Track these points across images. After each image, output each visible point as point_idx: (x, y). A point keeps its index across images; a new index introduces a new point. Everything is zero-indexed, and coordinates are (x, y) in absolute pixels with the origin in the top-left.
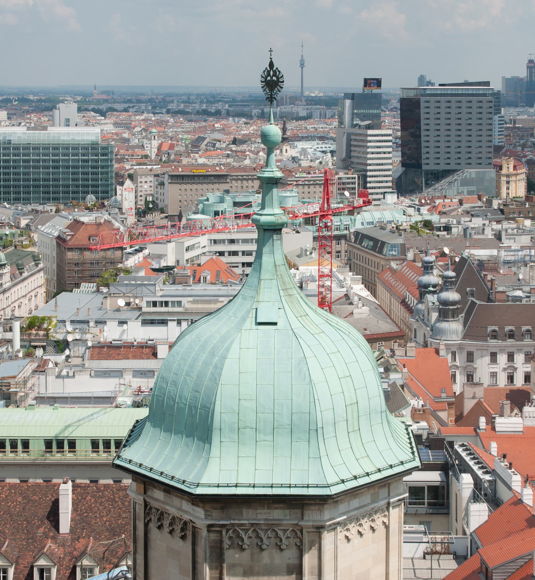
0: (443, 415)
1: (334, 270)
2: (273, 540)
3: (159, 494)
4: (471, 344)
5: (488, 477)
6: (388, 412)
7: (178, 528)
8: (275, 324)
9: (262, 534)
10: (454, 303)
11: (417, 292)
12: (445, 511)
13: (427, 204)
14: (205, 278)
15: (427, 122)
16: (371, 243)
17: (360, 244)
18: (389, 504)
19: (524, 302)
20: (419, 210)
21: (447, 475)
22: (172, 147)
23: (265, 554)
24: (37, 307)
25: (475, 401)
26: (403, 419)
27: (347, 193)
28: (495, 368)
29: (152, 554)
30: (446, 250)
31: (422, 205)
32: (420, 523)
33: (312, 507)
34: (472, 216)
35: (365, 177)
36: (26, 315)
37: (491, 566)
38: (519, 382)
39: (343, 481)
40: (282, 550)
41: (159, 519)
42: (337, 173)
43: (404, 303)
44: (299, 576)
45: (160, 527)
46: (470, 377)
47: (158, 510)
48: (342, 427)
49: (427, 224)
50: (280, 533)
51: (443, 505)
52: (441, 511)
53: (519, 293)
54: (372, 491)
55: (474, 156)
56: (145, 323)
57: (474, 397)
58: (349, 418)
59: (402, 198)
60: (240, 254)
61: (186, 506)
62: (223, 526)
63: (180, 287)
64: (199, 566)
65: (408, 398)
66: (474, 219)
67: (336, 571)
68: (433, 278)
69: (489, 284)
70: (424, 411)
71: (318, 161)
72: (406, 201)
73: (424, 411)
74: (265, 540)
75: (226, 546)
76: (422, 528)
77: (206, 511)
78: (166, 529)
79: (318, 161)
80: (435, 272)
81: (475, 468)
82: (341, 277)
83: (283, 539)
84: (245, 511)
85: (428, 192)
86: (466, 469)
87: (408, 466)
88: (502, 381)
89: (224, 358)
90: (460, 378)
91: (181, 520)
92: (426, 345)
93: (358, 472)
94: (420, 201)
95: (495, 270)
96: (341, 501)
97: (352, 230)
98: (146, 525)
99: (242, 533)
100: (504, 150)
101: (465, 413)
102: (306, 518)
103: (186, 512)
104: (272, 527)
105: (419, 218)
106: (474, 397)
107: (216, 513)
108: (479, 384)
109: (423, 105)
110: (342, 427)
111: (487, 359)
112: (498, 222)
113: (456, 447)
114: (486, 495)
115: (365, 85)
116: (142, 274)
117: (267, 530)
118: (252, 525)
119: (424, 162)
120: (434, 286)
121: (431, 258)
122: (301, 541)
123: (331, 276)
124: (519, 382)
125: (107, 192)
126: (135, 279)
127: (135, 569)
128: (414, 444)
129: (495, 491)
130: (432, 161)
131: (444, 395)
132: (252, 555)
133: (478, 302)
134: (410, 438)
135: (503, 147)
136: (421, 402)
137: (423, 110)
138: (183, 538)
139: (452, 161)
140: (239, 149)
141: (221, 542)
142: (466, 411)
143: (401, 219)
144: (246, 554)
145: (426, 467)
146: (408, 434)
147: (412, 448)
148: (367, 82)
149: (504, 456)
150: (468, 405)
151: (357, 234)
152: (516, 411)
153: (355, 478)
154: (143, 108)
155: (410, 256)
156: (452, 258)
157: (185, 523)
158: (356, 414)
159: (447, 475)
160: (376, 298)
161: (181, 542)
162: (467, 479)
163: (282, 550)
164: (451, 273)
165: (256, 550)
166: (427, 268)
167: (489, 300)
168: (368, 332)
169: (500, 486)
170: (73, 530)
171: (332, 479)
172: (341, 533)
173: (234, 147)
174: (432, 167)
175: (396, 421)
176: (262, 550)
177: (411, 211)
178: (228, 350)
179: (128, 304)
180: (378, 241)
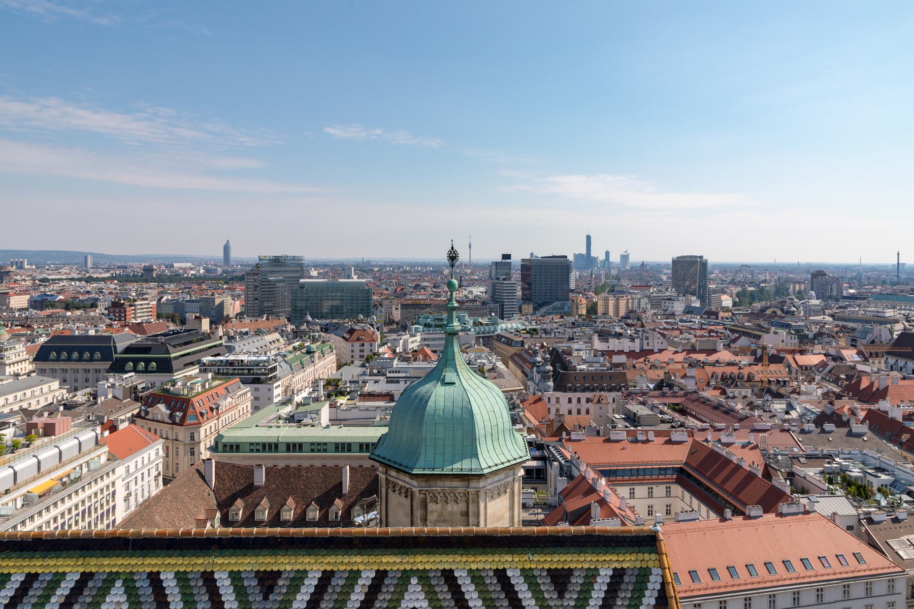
0: (544, 430)
2: (453, 498)
3: (393, 473)
4: (559, 394)
5: (567, 464)
7: (403, 491)
8: (454, 383)
9: (447, 495)
10: (549, 371)
11: (530, 366)
14: (419, 358)
20: (531, 323)
22: (402, 289)
23: (449, 505)
24: (332, 373)
26: (523, 433)
27: (493, 314)
29: (389, 505)
30: (545, 344)
32: (532, 488)
33: (474, 481)
35: (503, 305)
36: (326, 377)
41: (394, 487)
42: (488, 304)
43: (523, 372)
44: (466, 517)
45: (394, 491)
46: (558, 410)
47: (393, 482)
48: (489, 438)
50: (457, 494)
51: (544, 478)
54: (505, 472)
56: (388, 382)
58: (493, 433)
59: (522, 317)
61: (408, 479)
62: (427, 491)
63: (406, 363)
64: (414, 512)
68: (539, 359)
74: (449, 498)
75: (428, 501)
76: (532, 491)
77: (418, 482)
78: (397, 492)
80: (539, 355)
81: (560, 459)
84: (438, 482)
86: (556, 460)
87: (524, 459)
89: (427, 401)
91: (405, 487)
92: (534, 394)
93: (497, 462)
95: (570, 354)
97: (496, 333)
98: (387, 490)
99: (437, 494)
103: (408, 483)
105: (531, 327)
107: (423, 484)
110: (489, 438)
111: (567, 400)
114: (566, 473)
116: (386, 356)
117: (450, 493)
120: (539, 362)
121: (537, 348)
122: (468, 499)
125: (368, 313)
126: (383, 359)
127: (381, 513)
129: (571, 471)
131: (544, 421)
132: (442, 506)
138: (406, 497)
140: (437, 290)
141: (426, 499)
144: (439, 506)
145: (534, 458)
151: (498, 335)
154: (388, 269)
155: (526, 346)
156: (548, 348)
157: (407, 489)
160: (508, 368)
161: (405, 499)
163: (458, 503)
164: (548, 356)
165: (444, 503)
166: (535, 353)
169: (574, 468)
170: (350, 492)
173: (435, 290)
175: (517, 435)
176: (448, 503)
177: (526, 323)
178: (430, 397)
179: (379, 372)
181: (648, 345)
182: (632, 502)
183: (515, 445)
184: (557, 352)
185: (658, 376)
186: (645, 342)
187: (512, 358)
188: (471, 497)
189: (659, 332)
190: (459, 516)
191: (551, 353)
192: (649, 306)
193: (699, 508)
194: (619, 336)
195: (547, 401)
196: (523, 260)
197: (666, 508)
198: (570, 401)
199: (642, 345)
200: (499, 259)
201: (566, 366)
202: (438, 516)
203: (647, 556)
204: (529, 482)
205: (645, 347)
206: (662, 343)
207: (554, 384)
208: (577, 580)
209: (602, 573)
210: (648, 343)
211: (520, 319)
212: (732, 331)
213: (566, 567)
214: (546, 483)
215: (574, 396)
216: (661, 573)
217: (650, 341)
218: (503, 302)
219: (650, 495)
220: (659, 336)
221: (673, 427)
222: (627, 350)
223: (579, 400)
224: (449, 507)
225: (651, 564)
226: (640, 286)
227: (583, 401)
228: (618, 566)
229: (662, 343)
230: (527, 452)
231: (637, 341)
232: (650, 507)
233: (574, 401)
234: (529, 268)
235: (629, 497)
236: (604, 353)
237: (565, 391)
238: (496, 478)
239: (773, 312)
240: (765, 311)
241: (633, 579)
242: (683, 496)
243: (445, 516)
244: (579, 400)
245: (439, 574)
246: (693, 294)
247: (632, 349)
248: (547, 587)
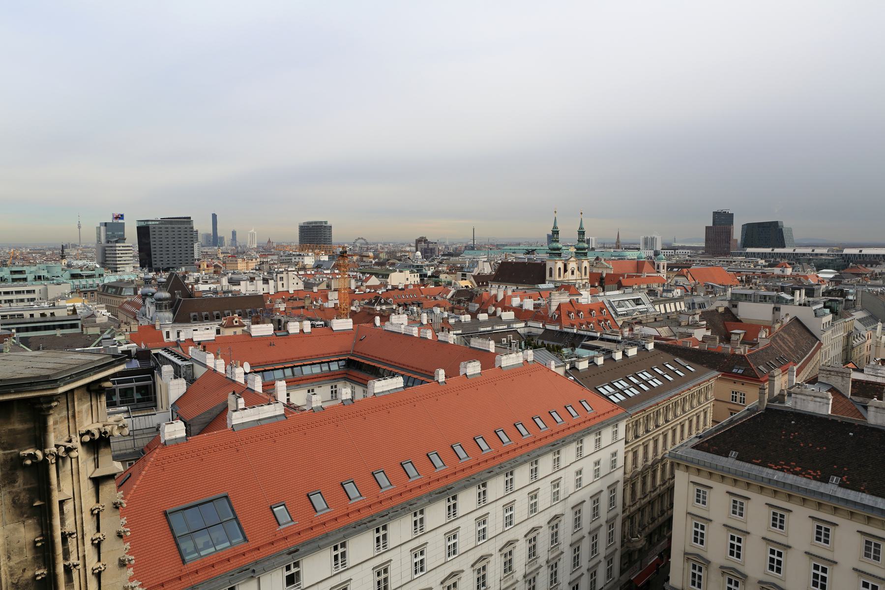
12: (153, 404)
52: (149, 405)
60: (26, 301)
180: (118, 287)
181: (283, 287)
186: (280, 283)
199: (276, 287)
205: (280, 289)
206: (297, 284)
210: (283, 284)
217: (285, 282)
229: (297, 284)
231: (271, 282)
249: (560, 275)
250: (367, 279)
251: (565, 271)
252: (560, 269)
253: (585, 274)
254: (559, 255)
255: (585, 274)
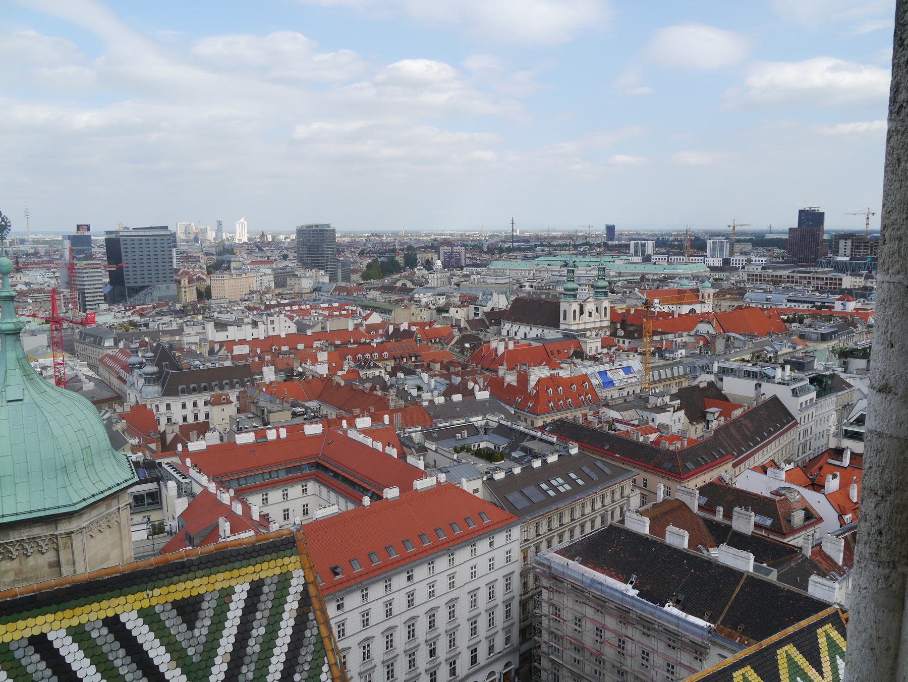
0: (153, 446)
1: (65, 359)
2: (36, 549)
6: (113, 450)
9: (26, 546)
13: (130, 309)
15: (126, 254)
16: (92, 339)
17: (84, 339)
18: (119, 508)
19: (201, 367)
21: (159, 484)
23: (30, 559)
25: (174, 434)
28: (184, 412)
31: (127, 310)
33: (63, 521)
34: (163, 315)
37: (192, 535)
38: (202, 418)
39: (84, 500)
40: (43, 554)
46: (169, 420)
48: (80, 465)
49: (132, 323)
50: (41, 543)
51: (158, 503)
53: (198, 363)
54: (106, 503)
55: (161, 275)
57: (173, 432)
65: (128, 439)
66: (164, 318)
67: (85, 559)
69: (177, 359)
70: (140, 446)
71: (46, 285)
72: (115, 308)
73: (140, 446)
79: (46, 285)
81: (177, 476)
82: (71, 364)
83: (43, 546)
84: (11, 533)
85: (131, 301)
86: (172, 478)
88: (191, 420)
90: (163, 421)
93: (95, 491)
94: (125, 308)
96: (85, 513)
99: (11, 549)
100: (181, 271)
101: (168, 443)
102: (59, 529)
104: (33, 540)
106: (173, 432)
108: (176, 423)
109: (122, 243)
110: (80, 465)
112: (181, 318)
113: (163, 465)
115: (78, 230)
117: (30, 542)
118: (18, 541)
119: (126, 281)
120: (140, 363)
122: (57, 545)
123: (63, 364)
124: (202, 418)
128: (133, 468)
130: (132, 281)
132: (20, 561)
133: (171, 371)
134: (130, 464)
135: (180, 269)
136: (137, 440)
137: (122, 246)
139: (147, 280)
142: (168, 443)
143: (113, 321)
144: (15, 564)
146: (129, 461)
147: (132, 470)
148: (79, 227)
149: (196, 466)
150: (170, 437)
152: (201, 437)
153: (93, 496)
158: (89, 455)
159: (159, 484)
162: (172, 485)
164: (151, 354)
165: (23, 557)
167: (178, 369)
168: (95, 399)
171: (76, 499)
172: (86, 534)
174: (132, 285)
181: (274, 330)
182: (266, 510)
183: (117, 467)
184: (163, 347)
185: (288, 365)
186: (270, 327)
187: (101, 360)
188: (61, 542)
189: (286, 315)
190: (47, 569)
191: (154, 350)
192: (272, 284)
193: (338, 502)
194: (238, 323)
195: (154, 410)
196: (108, 233)
197: (302, 508)
198: (184, 406)
199: (266, 331)
200: (73, 231)
201: (175, 365)
202: (16, 574)
203: (286, 560)
204: (139, 510)
205: (271, 333)
207: (163, 387)
208: (208, 608)
209: (238, 589)
211: (109, 309)
212: (364, 307)
213: (194, 593)
214: (162, 508)
215: (189, 400)
216: (302, 574)
217: (276, 325)
218: (84, 289)
219: (285, 496)
220: (286, 319)
221: (305, 419)
222: (249, 338)
223: (195, 404)
224: (31, 561)
225: (291, 568)
226: (261, 261)
227: (201, 404)
228: (256, 578)
230: (133, 473)
231: (261, 326)
232: (286, 511)
233: (190, 405)
234: (114, 246)
235: (261, 505)
236: (222, 344)
237: (177, 395)
238: (95, 513)
239: (402, 285)
240: (395, 283)
241: (274, 588)
242: (320, 493)
243: (26, 573)
244: (195, 404)
245: (26, 642)
246: (321, 267)
247: (255, 337)
248: (174, 624)
249: (575, 318)
250: (368, 316)
251: (582, 312)
252: (575, 311)
253: (605, 315)
254: (575, 296)
255: (605, 315)
